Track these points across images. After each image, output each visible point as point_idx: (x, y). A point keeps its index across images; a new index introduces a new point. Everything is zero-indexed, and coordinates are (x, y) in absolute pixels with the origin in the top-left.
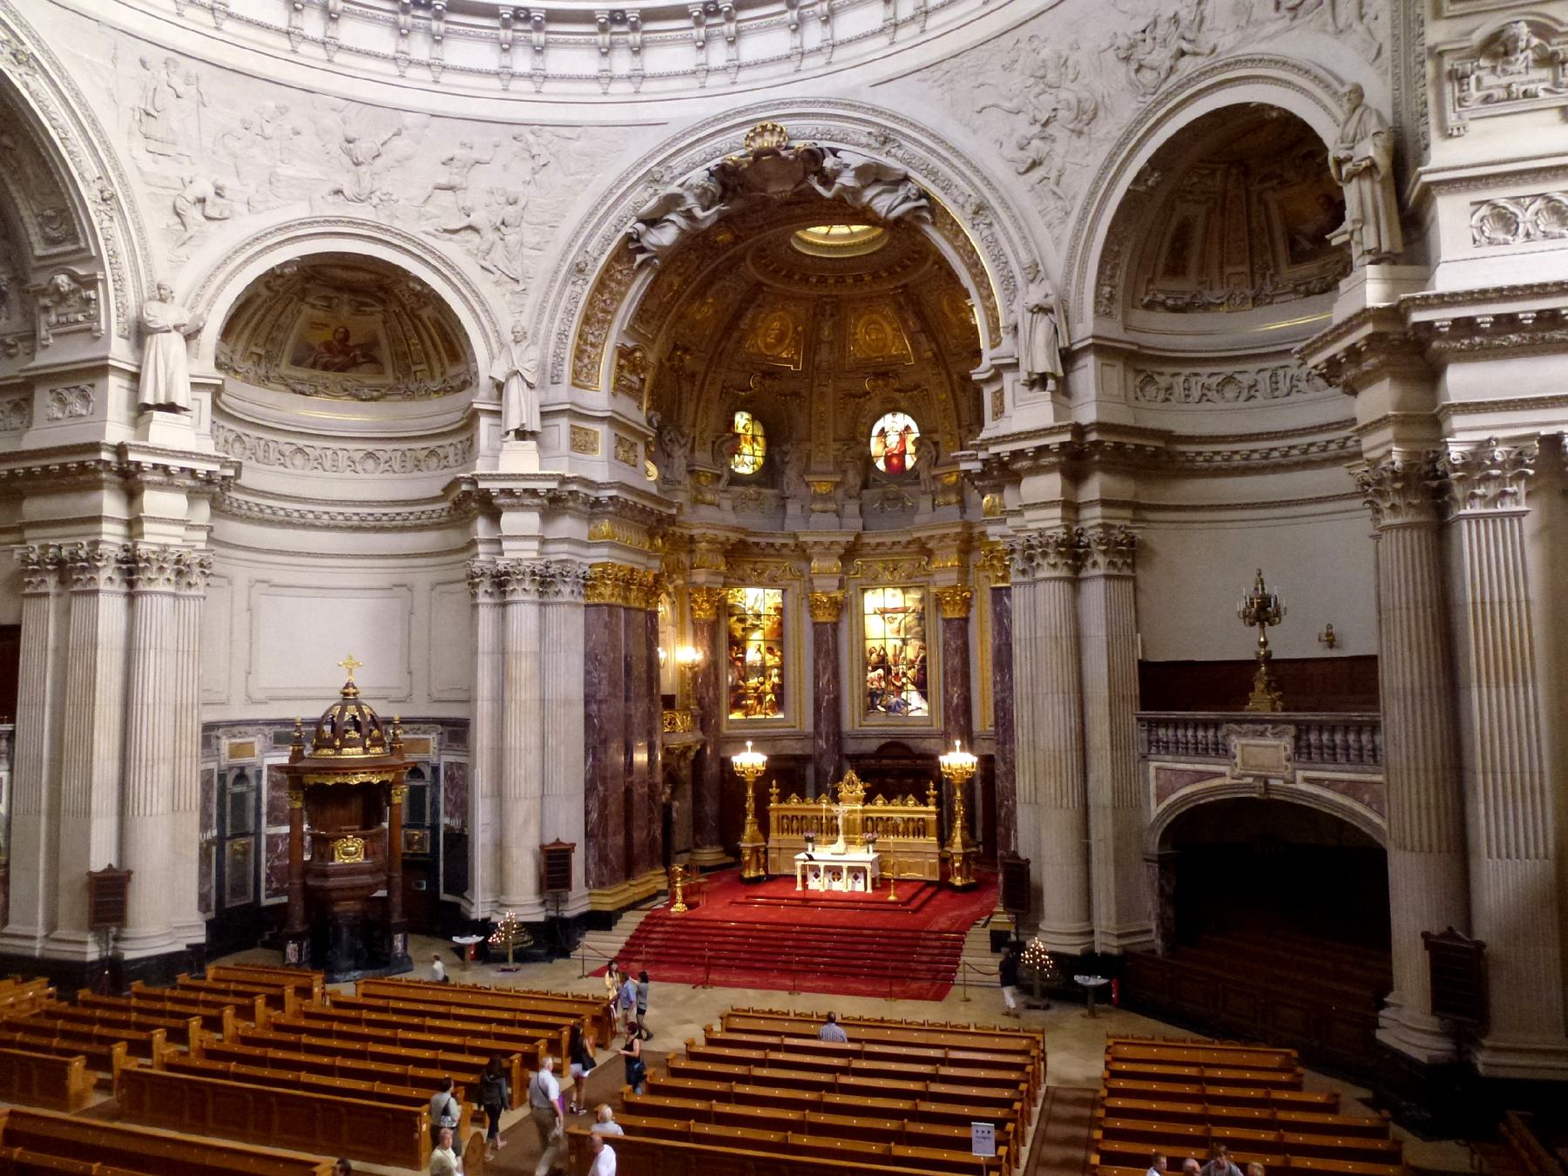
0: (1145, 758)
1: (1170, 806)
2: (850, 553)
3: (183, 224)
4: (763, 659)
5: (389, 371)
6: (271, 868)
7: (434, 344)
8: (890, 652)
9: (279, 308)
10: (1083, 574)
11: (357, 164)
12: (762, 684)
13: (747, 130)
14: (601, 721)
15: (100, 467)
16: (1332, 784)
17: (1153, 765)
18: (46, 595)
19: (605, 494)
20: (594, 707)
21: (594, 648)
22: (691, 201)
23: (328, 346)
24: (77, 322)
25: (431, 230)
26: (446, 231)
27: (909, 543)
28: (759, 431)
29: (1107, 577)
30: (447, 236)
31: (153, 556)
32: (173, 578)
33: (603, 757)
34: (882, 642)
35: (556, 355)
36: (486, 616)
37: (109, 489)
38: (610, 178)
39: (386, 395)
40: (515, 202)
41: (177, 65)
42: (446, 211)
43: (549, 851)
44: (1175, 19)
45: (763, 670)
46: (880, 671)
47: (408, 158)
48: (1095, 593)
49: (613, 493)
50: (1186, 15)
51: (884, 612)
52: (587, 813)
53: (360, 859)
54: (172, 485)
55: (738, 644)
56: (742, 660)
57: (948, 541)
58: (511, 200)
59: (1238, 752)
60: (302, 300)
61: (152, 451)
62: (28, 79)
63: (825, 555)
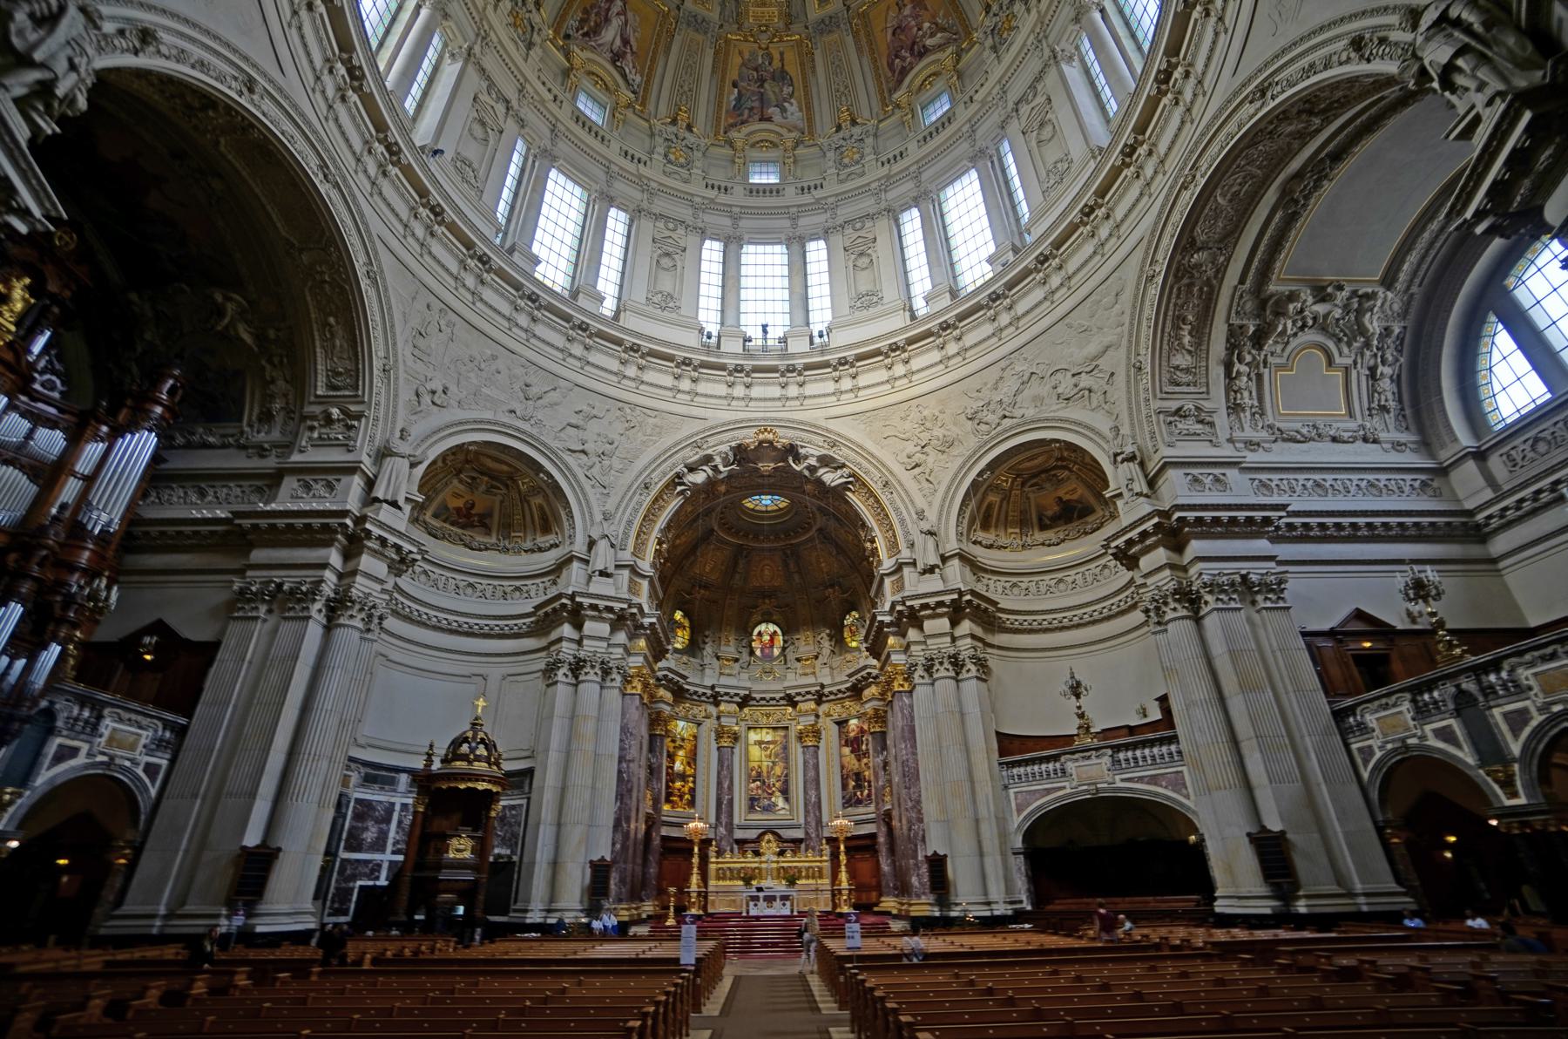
0: (1006, 787)
1: (1029, 814)
2: (745, 702)
5: (494, 535)
6: (337, 889)
7: (533, 522)
8: (764, 769)
9: (441, 476)
10: (960, 677)
13: (755, 430)
16: (1140, 780)
17: (1011, 791)
18: (256, 618)
19: (646, 621)
20: (624, 765)
22: (718, 460)
23: (458, 510)
24: (338, 439)
28: (687, 623)
29: (977, 678)
35: (625, 533)
36: (562, 691)
38: (670, 442)
42: (572, 439)
44: (1001, 402)
45: (683, 777)
47: (556, 404)
48: (971, 687)
50: (1005, 400)
51: (760, 743)
52: (613, 844)
53: (467, 855)
55: (671, 757)
56: (672, 768)
57: (809, 697)
59: (1074, 772)
60: (457, 475)
61: (381, 525)
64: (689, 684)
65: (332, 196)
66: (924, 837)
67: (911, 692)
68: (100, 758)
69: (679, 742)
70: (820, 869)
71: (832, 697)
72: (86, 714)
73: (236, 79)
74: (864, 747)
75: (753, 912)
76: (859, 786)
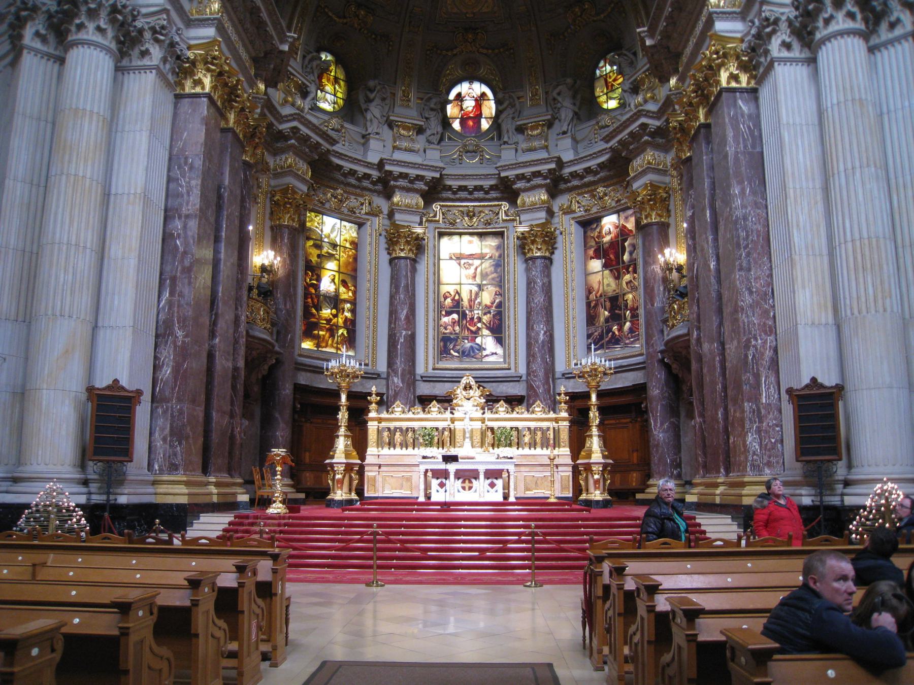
4: (337, 290)
8: (465, 297)
12: (335, 316)
14: (186, 244)
21: (183, 150)
27: (492, 188)
28: (341, 75)
33: (186, 291)
34: (457, 287)
43: (100, 396)
45: (335, 301)
46: (455, 316)
51: (459, 257)
52: (156, 368)
55: (314, 270)
56: (317, 287)
57: (538, 181)
63: (408, 190)
64: (340, 156)
66: (774, 364)
67: (753, 92)
69: (326, 249)
70: (556, 432)
71: (576, 183)
74: (626, 257)
75: (438, 496)
76: (616, 317)
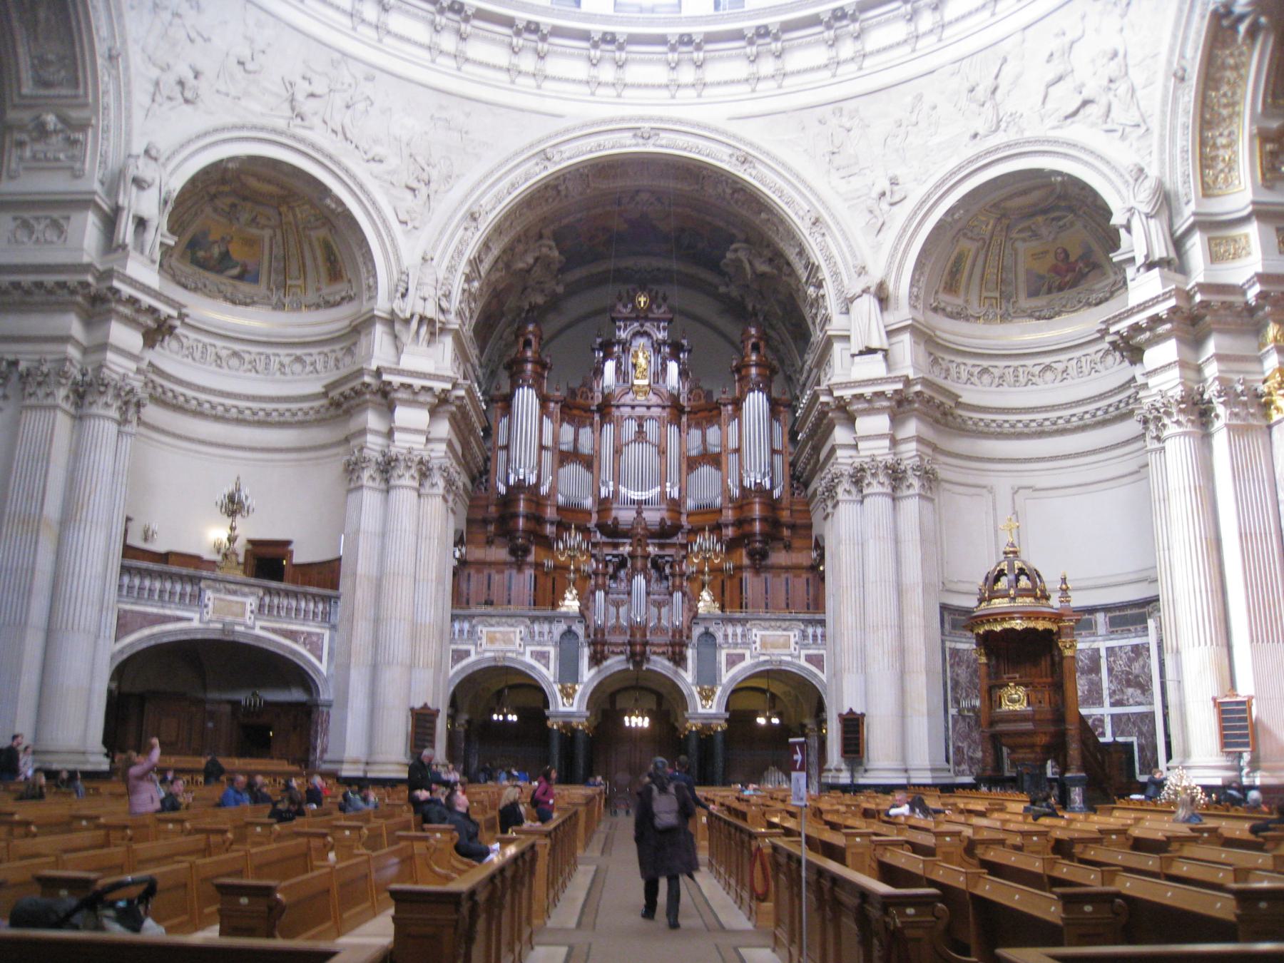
3: (876, 217)
11: (983, 105)
15: (826, 409)
19: (1252, 294)
23: (1055, 269)
25: (1056, 123)
26: (1067, 117)
30: (1069, 121)
31: (866, 466)
32: (887, 482)
37: (842, 425)
39: (1112, 293)
40: (1115, 55)
41: (841, 110)
42: (1065, 99)
47: (1018, 77)
49: (1257, 289)
54: (874, 409)
58: (1110, 56)
62: (749, 170)
65: (664, 142)
68: (762, 658)
72: (739, 630)
73: (537, 164)
